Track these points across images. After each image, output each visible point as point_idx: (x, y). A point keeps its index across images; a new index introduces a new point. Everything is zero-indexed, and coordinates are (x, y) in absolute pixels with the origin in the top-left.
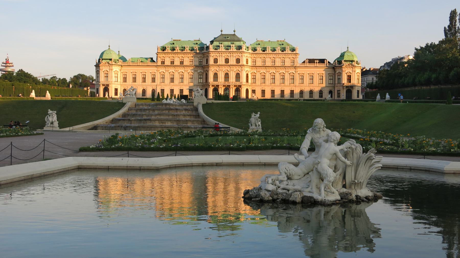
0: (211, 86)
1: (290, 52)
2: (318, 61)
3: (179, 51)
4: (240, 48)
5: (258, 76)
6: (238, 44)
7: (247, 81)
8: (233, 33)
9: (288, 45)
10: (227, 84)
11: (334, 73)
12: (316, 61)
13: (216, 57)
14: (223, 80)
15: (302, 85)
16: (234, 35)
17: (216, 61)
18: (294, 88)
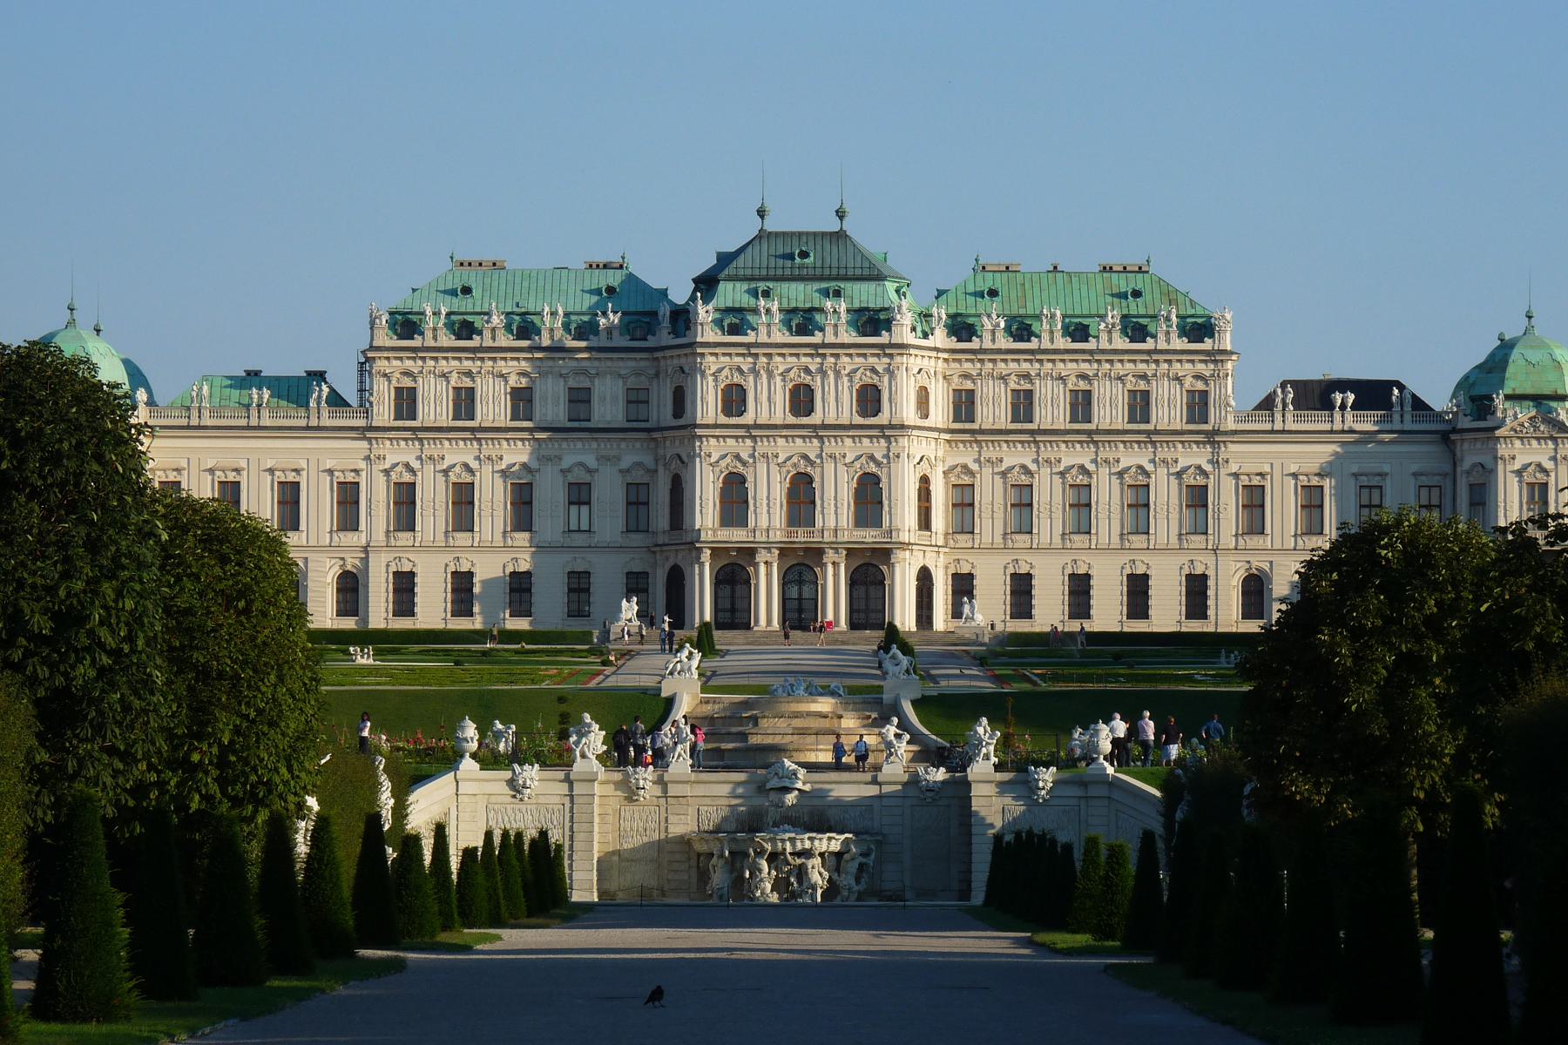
0: (706, 555)
1: (1179, 343)
2: (1351, 397)
3: (504, 340)
4: (873, 321)
5: (991, 496)
6: (863, 294)
7: (925, 522)
8: (833, 225)
9: (1171, 296)
10: (801, 536)
11: (1447, 468)
12: (1338, 397)
13: (737, 379)
14: (779, 517)
15: (1255, 541)
16: (840, 236)
17: (734, 400)
18: (1210, 559)
